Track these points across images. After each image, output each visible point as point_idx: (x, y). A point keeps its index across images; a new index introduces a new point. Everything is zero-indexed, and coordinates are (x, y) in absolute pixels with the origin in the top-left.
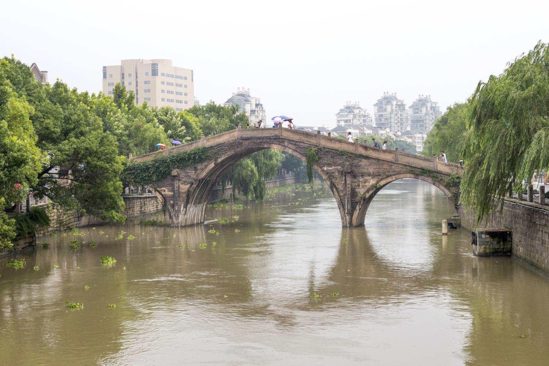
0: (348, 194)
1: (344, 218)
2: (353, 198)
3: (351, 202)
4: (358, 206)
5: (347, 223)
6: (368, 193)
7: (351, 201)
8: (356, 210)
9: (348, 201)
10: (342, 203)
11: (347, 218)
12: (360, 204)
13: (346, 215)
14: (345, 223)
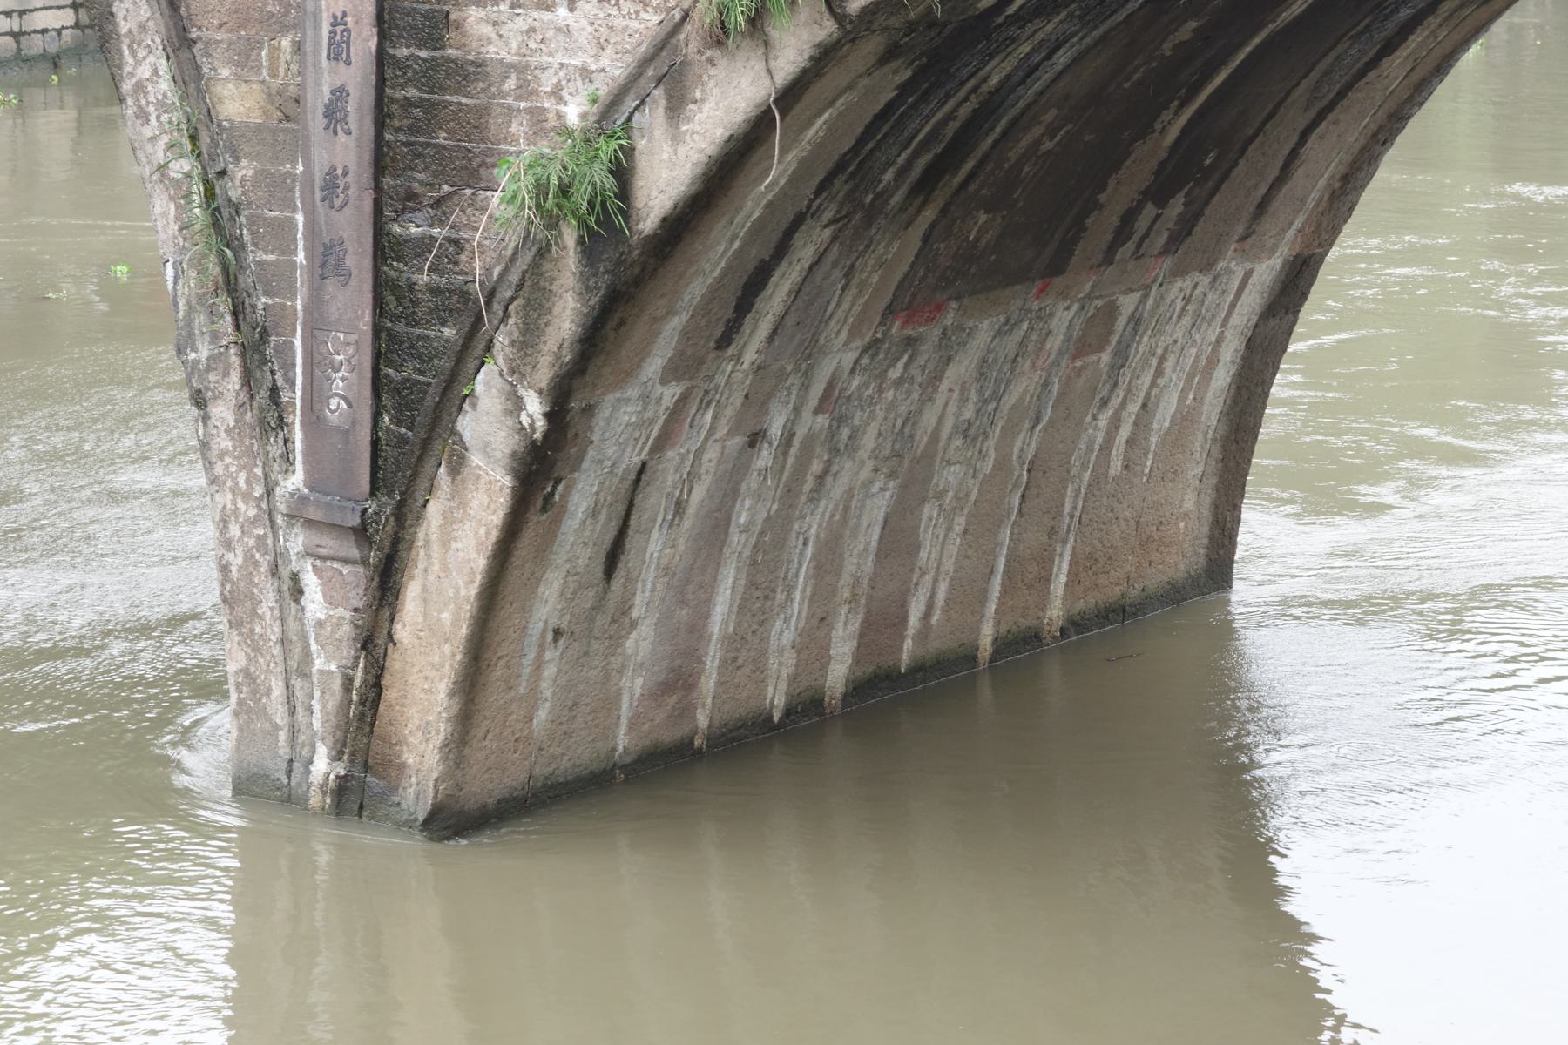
0: (334, 114)
1: (268, 603)
2: (410, 199)
3: (381, 286)
4: (487, 384)
5: (320, 714)
6: (677, 106)
7: (384, 248)
8: (458, 464)
9: (326, 259)
10: (230, 283)
11: (315, 602)
12: (528, 341)
13: (295, 541)
14: (279, 715)
